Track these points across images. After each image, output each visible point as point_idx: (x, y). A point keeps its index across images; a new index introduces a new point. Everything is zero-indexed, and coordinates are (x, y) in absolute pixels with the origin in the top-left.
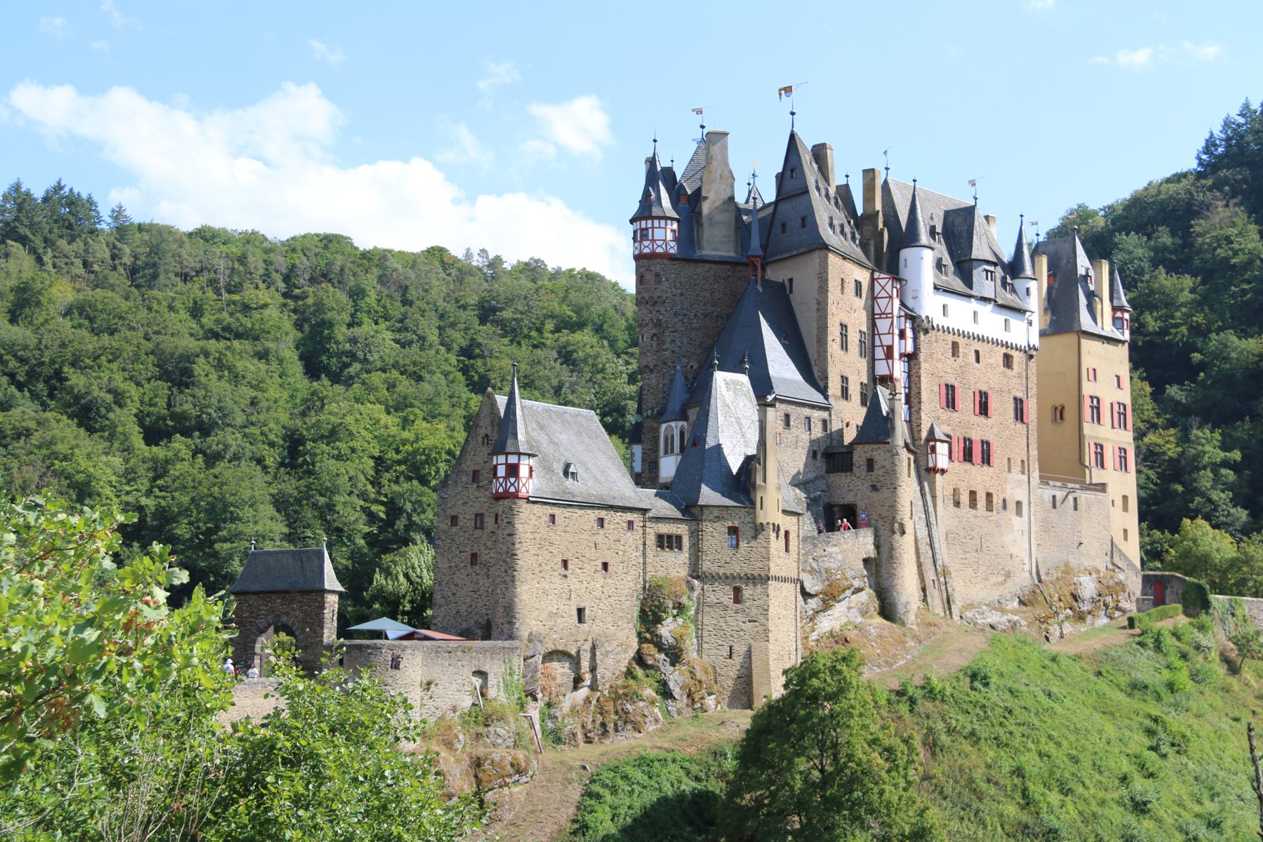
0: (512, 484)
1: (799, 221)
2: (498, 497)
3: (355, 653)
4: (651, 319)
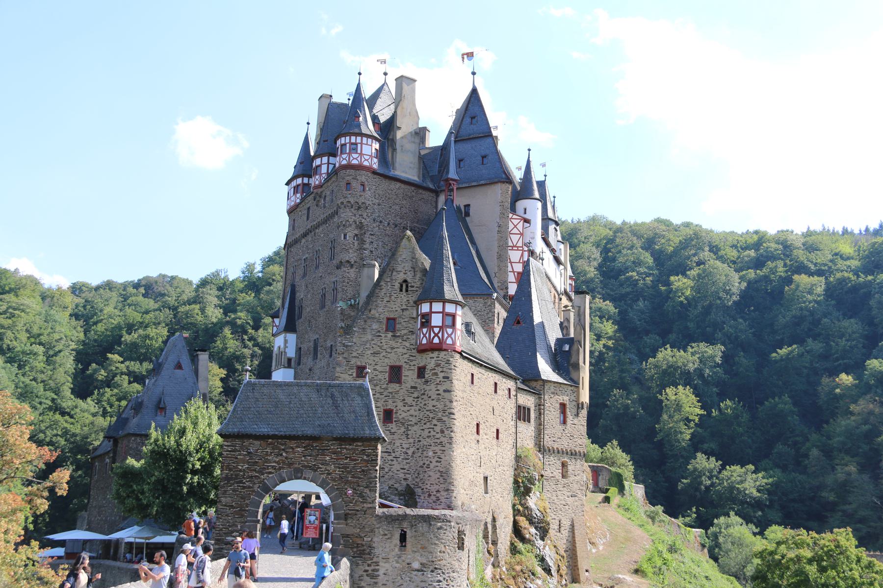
0: (449, 336)
1: (480, 158)
2: (422, 350)
3: (422, 527)
4: (355, 222)
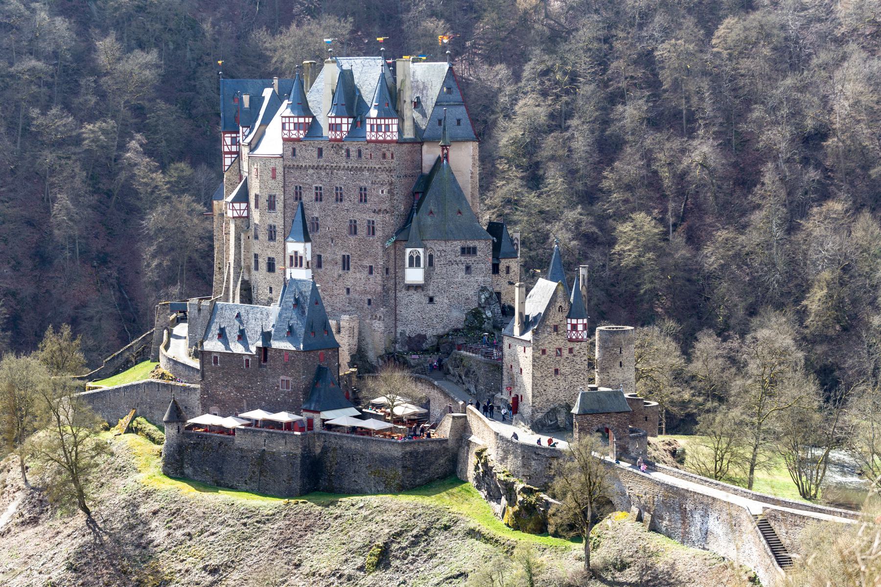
2: (571, 340)
